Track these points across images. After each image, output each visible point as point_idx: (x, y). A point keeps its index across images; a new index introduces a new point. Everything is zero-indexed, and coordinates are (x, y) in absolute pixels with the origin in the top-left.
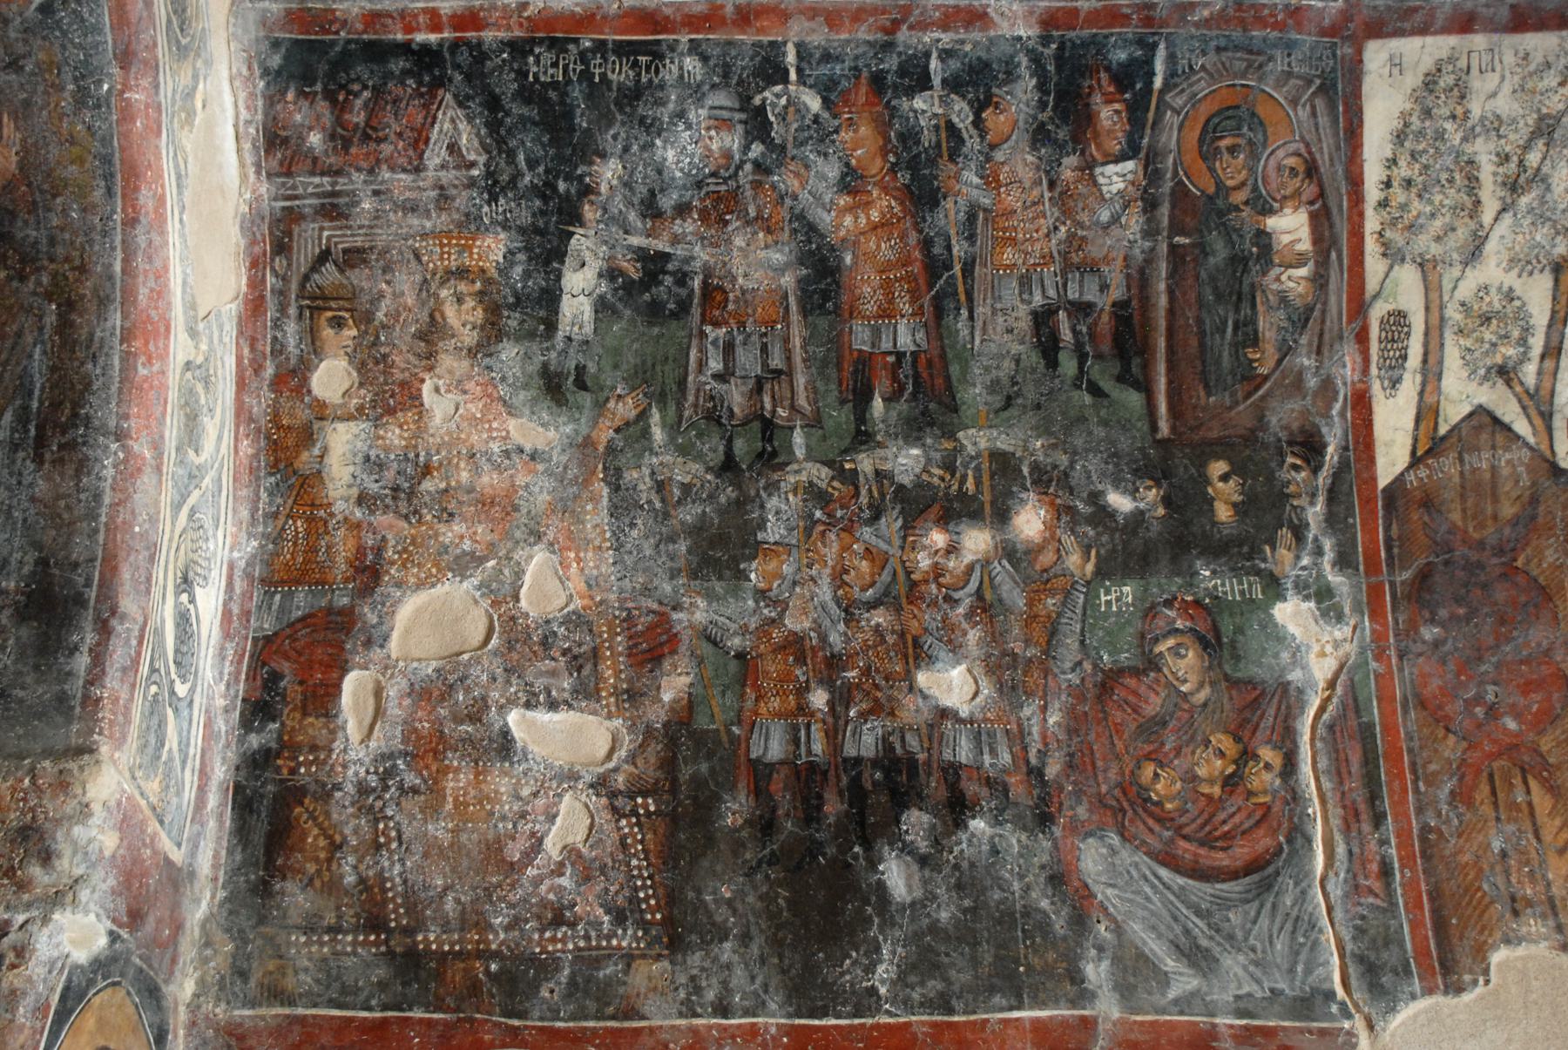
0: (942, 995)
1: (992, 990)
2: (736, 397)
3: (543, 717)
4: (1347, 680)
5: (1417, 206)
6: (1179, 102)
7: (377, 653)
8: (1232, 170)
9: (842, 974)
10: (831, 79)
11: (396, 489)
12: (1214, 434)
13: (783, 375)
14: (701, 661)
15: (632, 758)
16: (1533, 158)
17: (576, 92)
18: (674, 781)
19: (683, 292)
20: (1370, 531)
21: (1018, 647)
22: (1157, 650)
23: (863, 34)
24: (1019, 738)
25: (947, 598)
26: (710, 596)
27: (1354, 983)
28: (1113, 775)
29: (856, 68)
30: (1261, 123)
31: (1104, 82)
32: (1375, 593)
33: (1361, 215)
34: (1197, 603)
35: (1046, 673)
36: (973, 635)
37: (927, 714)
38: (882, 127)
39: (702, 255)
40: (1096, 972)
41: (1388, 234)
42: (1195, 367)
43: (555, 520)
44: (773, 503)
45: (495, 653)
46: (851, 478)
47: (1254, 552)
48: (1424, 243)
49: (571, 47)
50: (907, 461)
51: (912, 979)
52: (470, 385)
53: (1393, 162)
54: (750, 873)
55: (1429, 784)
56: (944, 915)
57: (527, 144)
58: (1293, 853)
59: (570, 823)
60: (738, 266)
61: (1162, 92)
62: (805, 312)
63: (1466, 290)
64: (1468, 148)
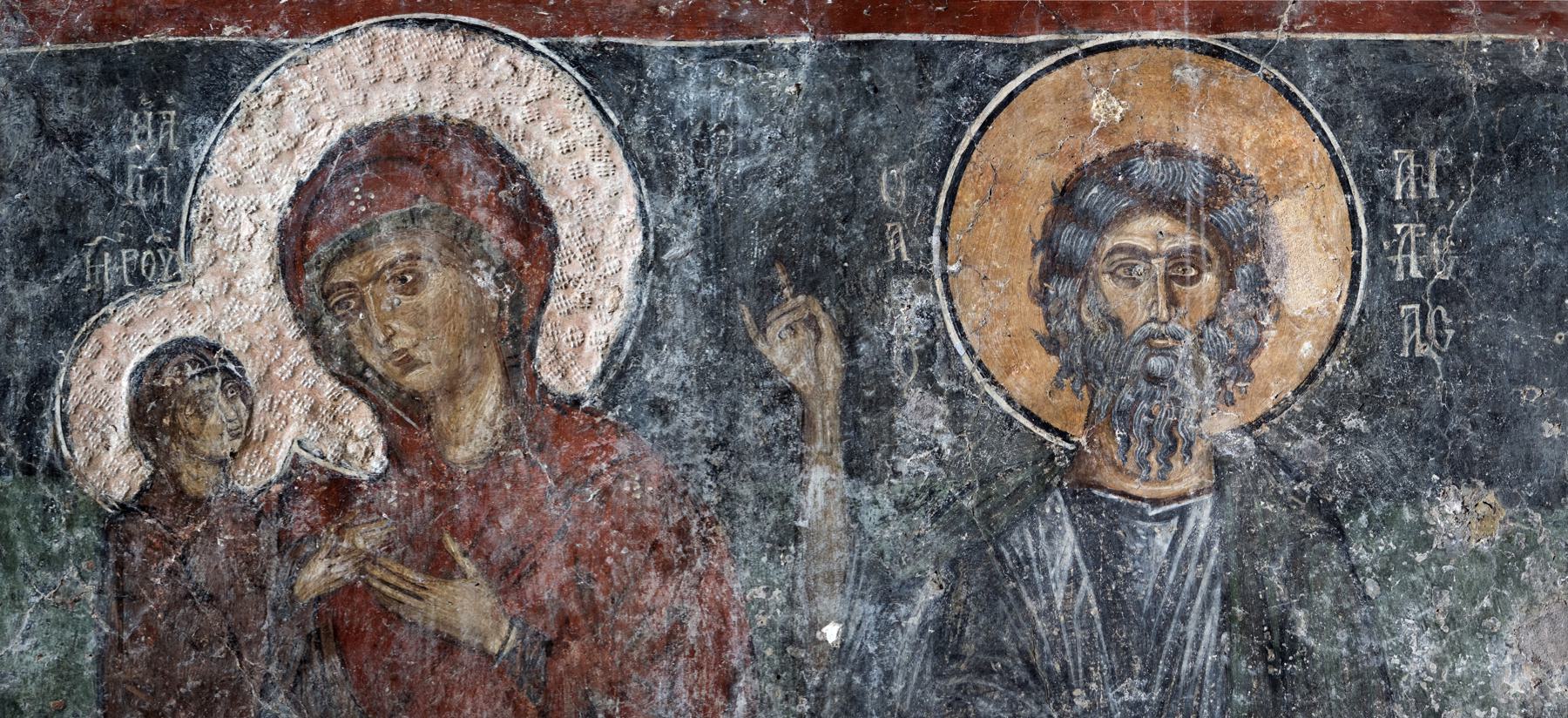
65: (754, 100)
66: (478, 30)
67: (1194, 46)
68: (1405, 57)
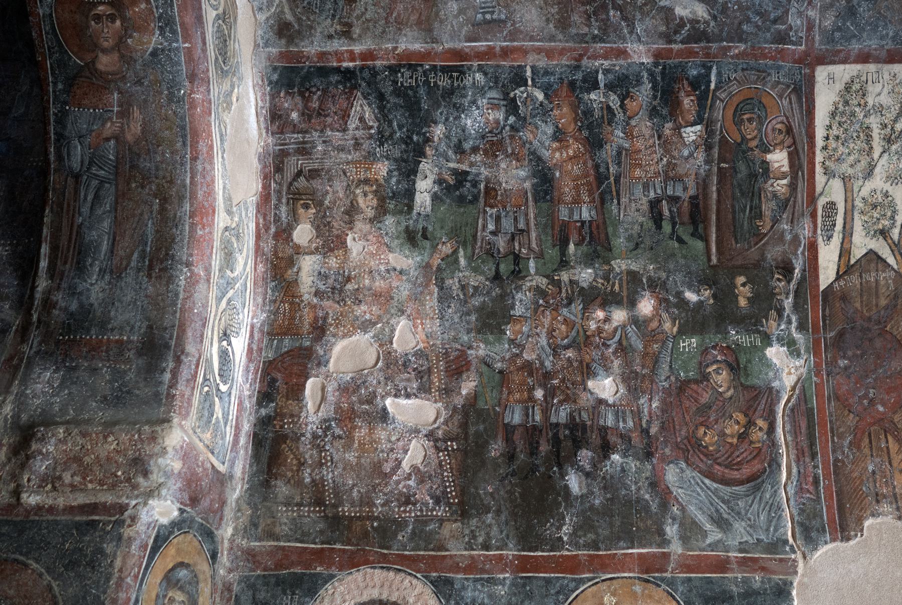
0: (594, 541)
1: (619, 539)
2: (501, 243)
3: (403, 401)
4: (801, 386)
5: (841, 149)
6: (723, 96)
7: (323, 369)
8: (750, 130)
9: (546, 530)
10: (549, 84)
11: (333, 288)
12: (739, 263)
13: (525, 232)
14: (481, 375)
15: (446, 423)
17: (422, 91)
18: (466, 434)
19: (476, 191)
21: (638, 369)
22: (708, 371)
23: (565, 61)
24: (637, 414)
25: (604, 344)
26: (487, 342)
27: (798, 536)
28: (683, 433)
29: (561, 79)
30: (764, 107)
31: (686, 86)
32: (817, 343)
33: (814, 153)
34: (728, 347)
35: (652, 382)
36: (617, 363)
37: (592, 402)
38: (574, 108)
39: (485, 172)
40: (671, 530)
41: (827, 163)
42: (730, 229)
43: (411, 304)
44: (519, 296)
45: (380, 370)
46: (558, 284)
47: (758, 322)
48: (845, 168)
49: (419, 68)
50: (586, 275)
51: (579, 533)
52: (370, 237)
53: (830, 127)
54: (502, 480)
55: (839, 438)
56: (597, 502)
57: (398, 117)
58: (771, 472)
59: (415, 453)
60: (502, 178)
61: (714, 90)
62: (536, 201)
63: (865, 192)
64: (867, 121)
65: (490, 596)
66: (400, 570)
67: (639, 578)
68: (712, 582)
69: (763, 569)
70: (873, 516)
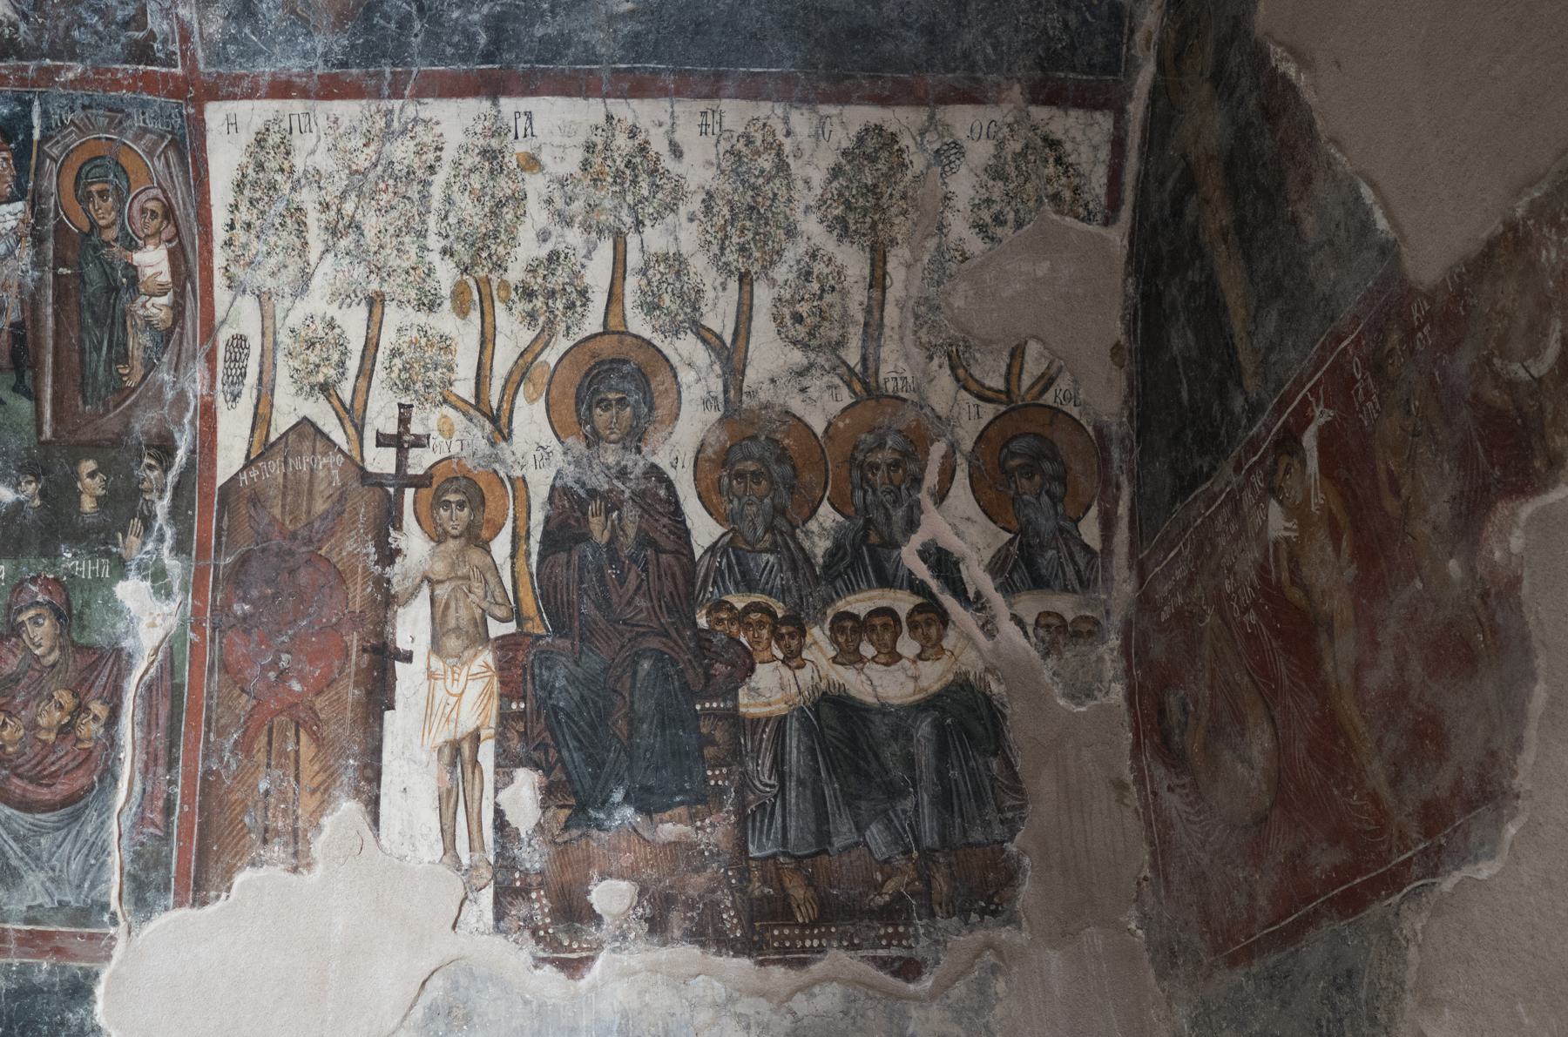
5: (256, 245)
6: (55, 152)
8: (104, 211)
16: (349, 207)
20: (205, 521)
22: (20, 619)
27: (125, 896)
30: (124, 171)
32: (201, 574)
33: (210, 252)
34: (56, 580)
41: (232, 269)
42: (77, 380)
48: (260, 278)
53: (235, 207)
55: (219, 734)
58: (102, 790)
63: (295, 319)
64: (297, 197)
69: (58, 951)
70: (253, 865)
